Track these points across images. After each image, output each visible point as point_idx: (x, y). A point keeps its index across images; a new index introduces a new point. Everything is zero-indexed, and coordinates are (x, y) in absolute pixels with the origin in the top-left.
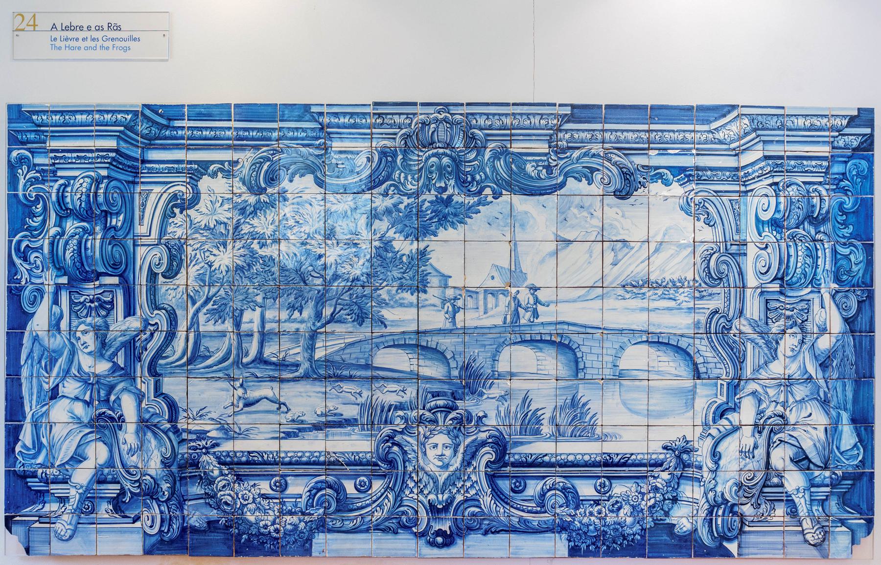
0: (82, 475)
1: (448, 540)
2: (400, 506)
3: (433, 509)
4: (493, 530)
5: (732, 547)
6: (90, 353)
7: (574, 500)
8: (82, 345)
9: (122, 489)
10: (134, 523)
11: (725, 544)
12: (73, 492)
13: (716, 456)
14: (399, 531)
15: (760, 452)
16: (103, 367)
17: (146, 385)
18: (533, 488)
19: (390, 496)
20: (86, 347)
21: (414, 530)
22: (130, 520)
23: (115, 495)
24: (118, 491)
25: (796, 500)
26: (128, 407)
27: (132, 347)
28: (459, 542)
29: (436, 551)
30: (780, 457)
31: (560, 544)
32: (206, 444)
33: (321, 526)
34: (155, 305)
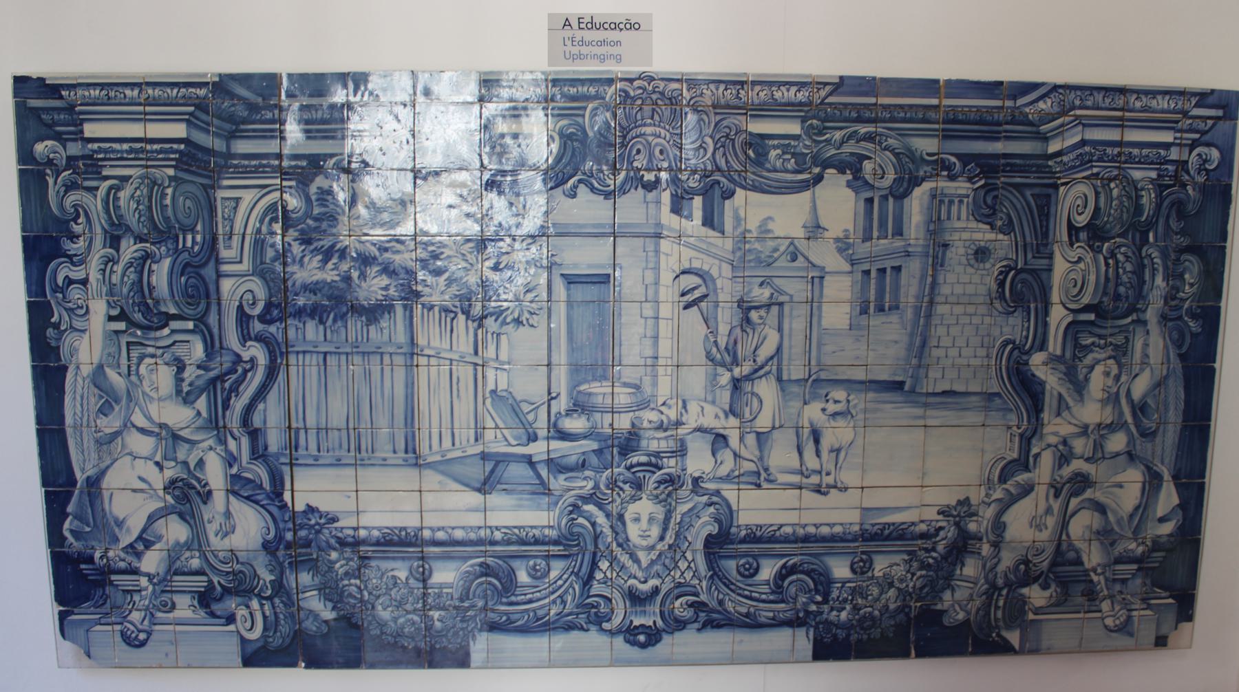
1: (653, 637)
2: (589, 597)
5: (1014, 637)
9: (210, 582)
10: (227, 625)
13: (999, 526)
19: (577, 587)
21: (606, 626)
22: (223, 621)
23: (203, 589)
24: (206, 584)
25: (1095, 578)
26: (215, 475)
34: (245, 337)
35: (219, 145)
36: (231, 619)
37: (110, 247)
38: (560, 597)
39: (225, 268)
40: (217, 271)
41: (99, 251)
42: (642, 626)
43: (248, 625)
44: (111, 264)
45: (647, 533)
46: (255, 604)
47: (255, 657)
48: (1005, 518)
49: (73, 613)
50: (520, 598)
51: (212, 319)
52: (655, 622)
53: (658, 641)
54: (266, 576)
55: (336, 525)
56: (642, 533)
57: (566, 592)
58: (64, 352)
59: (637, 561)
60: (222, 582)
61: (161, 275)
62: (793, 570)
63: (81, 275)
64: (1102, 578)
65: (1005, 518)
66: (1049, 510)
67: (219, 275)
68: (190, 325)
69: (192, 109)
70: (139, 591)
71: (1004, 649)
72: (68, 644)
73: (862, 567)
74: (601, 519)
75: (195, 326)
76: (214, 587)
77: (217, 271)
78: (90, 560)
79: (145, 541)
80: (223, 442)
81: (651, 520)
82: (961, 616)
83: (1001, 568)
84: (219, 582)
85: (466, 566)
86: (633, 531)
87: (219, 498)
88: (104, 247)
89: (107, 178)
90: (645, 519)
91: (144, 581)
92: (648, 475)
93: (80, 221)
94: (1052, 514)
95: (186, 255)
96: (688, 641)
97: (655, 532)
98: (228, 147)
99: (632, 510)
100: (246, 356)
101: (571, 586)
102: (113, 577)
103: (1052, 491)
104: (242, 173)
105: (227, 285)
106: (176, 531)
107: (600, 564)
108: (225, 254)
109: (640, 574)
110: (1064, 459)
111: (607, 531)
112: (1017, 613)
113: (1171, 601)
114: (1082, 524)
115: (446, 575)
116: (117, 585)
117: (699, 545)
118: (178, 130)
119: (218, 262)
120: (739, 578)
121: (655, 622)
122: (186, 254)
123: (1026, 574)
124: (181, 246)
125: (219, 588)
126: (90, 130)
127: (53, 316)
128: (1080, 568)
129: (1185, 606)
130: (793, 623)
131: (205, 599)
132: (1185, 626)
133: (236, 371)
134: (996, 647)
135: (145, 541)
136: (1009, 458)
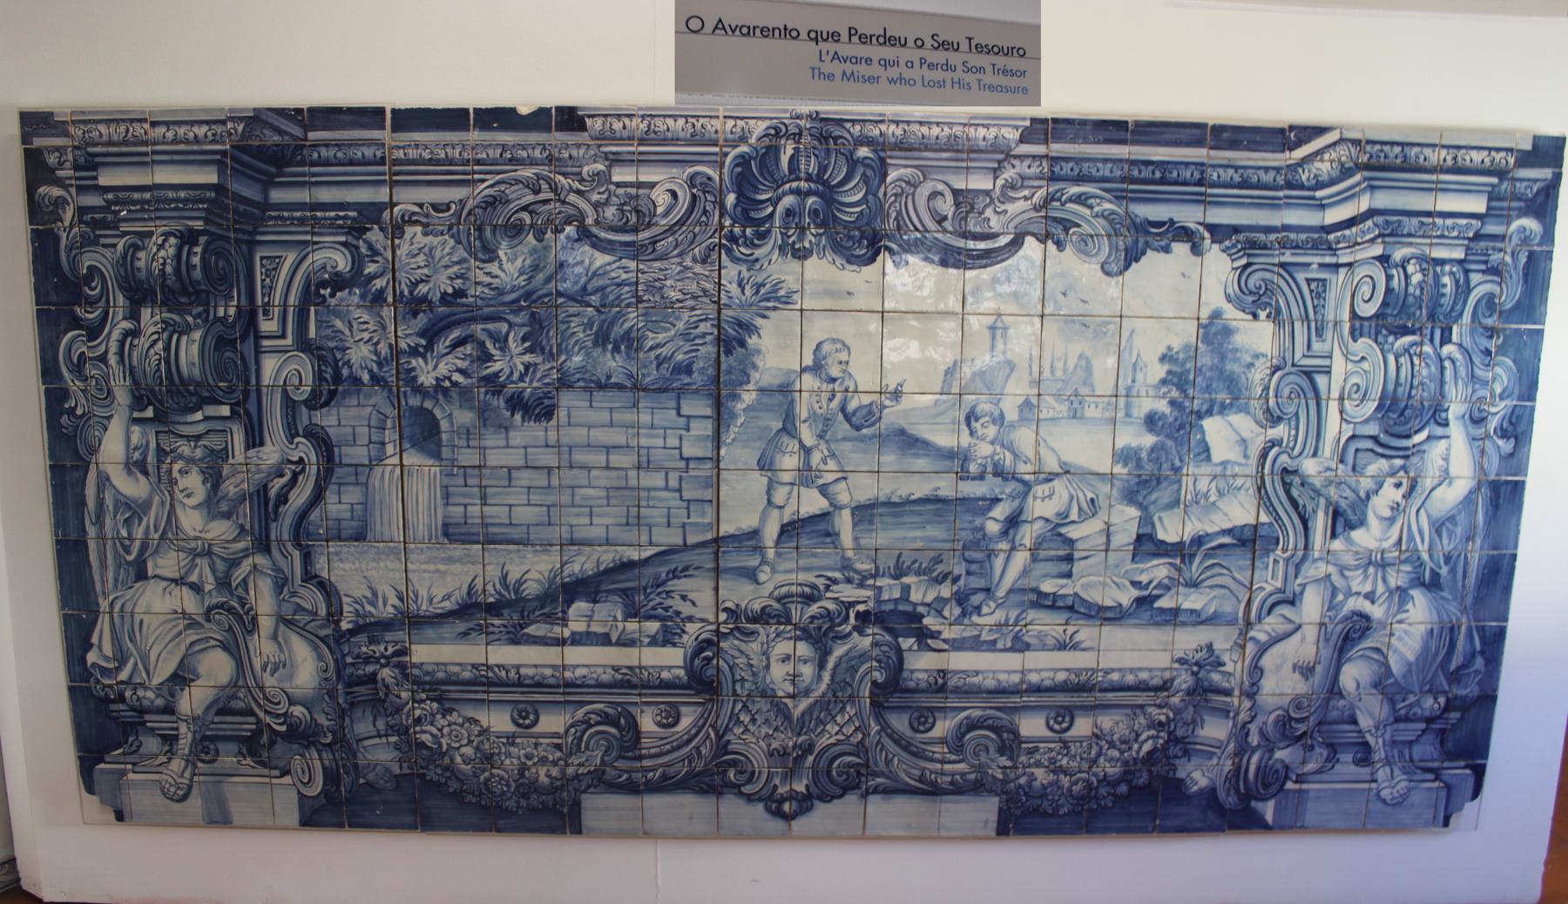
1: (805, 803)
6: (194, 508)
7: (1010, 742)
8: (182, 491)
11: (1253, 804)
12: (183, 728)
16: (220, 530)
20: (188, 496)
21: (747, 789)
24: (254, 727)
27: (265, 503)
30: (1354, 674)
31: (987, 809)
32: (386, 649)
33: (601, 781)
47: (316, 815)
49: (102, 760)
52: (807, 787)
53: (809, 809)
72: (95, 799)
78: (121, 698)
79: (181, 678)
89: (125, 234)
93: (94, 284)
105: (270, 365)
116: (153, 729)
119: (258, 337)
124: (211, 317)
135: (181, 678)
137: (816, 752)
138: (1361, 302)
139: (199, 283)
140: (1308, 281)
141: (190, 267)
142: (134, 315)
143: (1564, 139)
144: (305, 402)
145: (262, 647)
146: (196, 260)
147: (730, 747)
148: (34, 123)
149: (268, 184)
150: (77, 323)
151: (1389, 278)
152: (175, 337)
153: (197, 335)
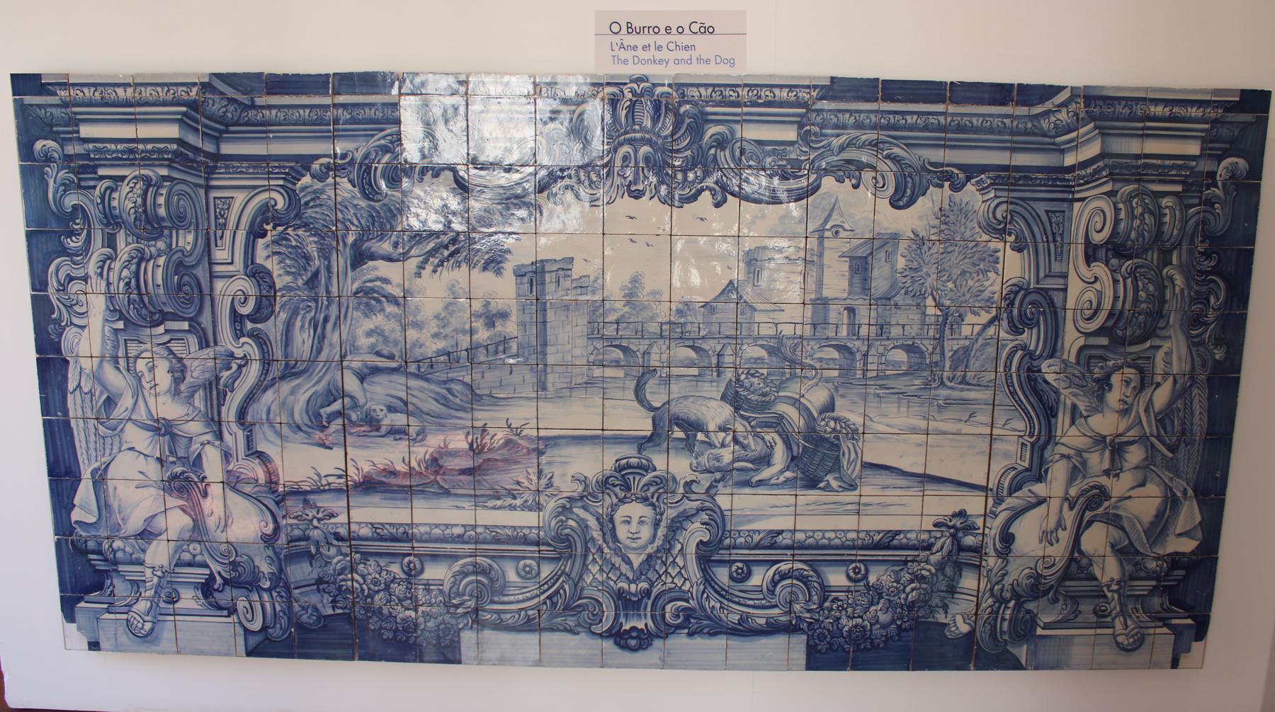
0: (158, 554)
3: (626, 602)
4: (705, 631)
5: (1022, 652)
9: (212, 573)
10: (229, 616)
13: (1007, 538)
14: (579, 629)
15: (1065, 536)
17: (234, 437)
18: (759, 578)
19: (567, 587)
22: (225, 613)
25: (1109, 595)
28: (658, 643)
29: (627, 656)
35: (209, 147)
36: (232, 611)
37: (108, 247)
38: (549, 597)
39: (218, 268)
40: (211, 272)
41: (99, 250)
42: (634, 628)
43: (250, 616)
44: (108, 262)
45: (636, 536)
46: (255, 597)
48: (1011, 530)
50: (511, 598)
51: (206, 320)
52: (646, 625)
53: (650, 645)
54: (265, 568)
55: (333, 520)
56: (631, 535)
57: (557, 592)
58: (64, 346)
59: (629, 562)
60: (223, 573)
61: (156, 274)
62: (784, 576)
63: (81, 273)
64: (1116, 596)
65: (1011, 530)
66: (1060, 525)
67: (212, 276)
68: (185, 325)
69: (184, 109)
70: (144, 581)
71: (1016, 665)
73: (857, 578)
74: (592, 522)
75: (190, 326)
76: (215, 578)
77: (211, 272)
79: (147, 535)
80: (220, 436)
81: (641, 522)
82: (965, 628)
83: (1008, 580)
84: (219, 573)
85: (457, 566)
86: (622, 532)
87: (216, 490)
88: (103, 247)
90: (635, 521)
91: (148, 572)
92: (637, 478)
94: (1065, 529)
95: (179, 254)
96: (680, 641)
97: (646, 532)
98: (218, 149)
99: (624, 511)
100: (239, 353)
101: (562, 587)
102: (121, 568)
103: (1066, 505)
104: (234, 173)
105: (219, 285)
106: (177, 522)
107: (590, 567)
108: (220, 255)
109: (630, 575)
110: (1077, 471)
111: (596, 534)
112: (1024, 629)
113: (1189, 621)
114: (1096, 539)
115: (435, 572)
117: (691, 549)
118: (172, 131)
119: (211, 264)
120: (732, 584)
121: (646, 625)
122: (179, 254)
123: (1036, 588)
124: (174, 246)
125: (219, 580)
126: (86, 131)
127: (53, 313)
128: (1095, 583)
129: (1201, 630)
130: (790, 629)
131: (207, 588)
132: (1196, 646)
133: (231, 368)
134: (1002, 660)
136: (1020, 468)
137: (653, 597)
138: (1094, 233)
139: (163, 219)
140: (1047, 212)
141: (155, 205)
142: (111, 242)
143: (1269, 93)
144: (248, 316)
145: (213, 505)
146: (161, 200)
147: (585, 592)
148: (23, 84)
149: (217, 140)
150: (64, 252)
151: (1117, 210)
152: (143, 265)
153: (161, 261)
